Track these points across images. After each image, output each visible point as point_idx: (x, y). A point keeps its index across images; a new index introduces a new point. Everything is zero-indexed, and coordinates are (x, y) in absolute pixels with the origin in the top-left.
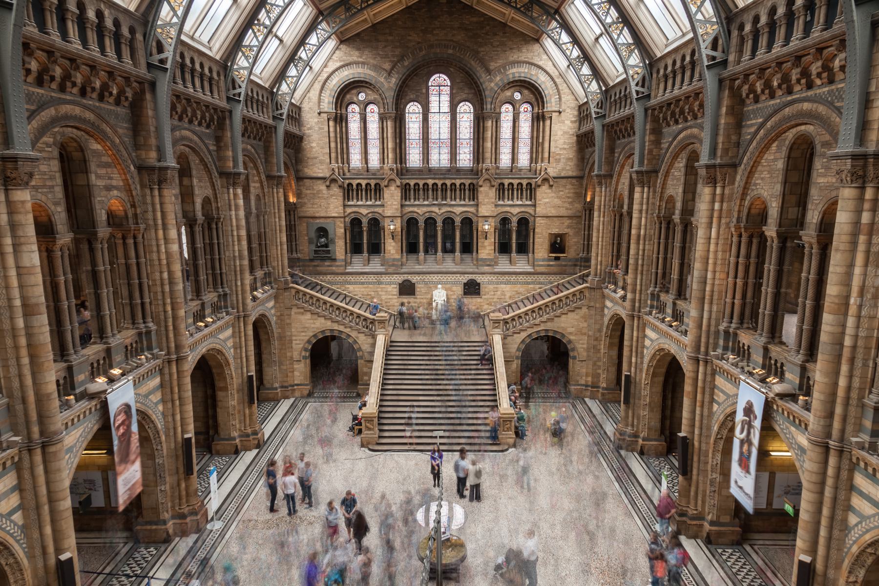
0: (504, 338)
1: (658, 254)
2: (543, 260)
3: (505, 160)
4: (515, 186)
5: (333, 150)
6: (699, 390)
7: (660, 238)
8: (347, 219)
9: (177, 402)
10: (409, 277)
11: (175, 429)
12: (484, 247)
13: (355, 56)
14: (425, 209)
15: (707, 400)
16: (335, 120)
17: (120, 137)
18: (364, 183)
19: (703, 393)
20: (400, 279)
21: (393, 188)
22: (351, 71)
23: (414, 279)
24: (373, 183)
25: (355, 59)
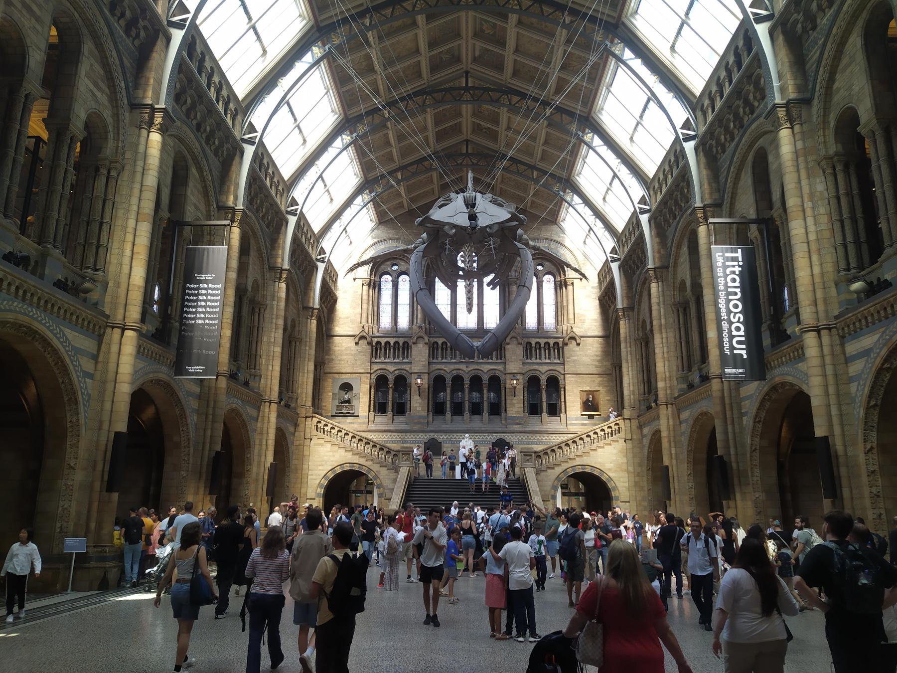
0: (537, 474)
1: (681, 339)
2: (577, 419)
3: (531, 321)
4: (542, 345)
5: (365, 311)
6: (727, 407)
7: (679, 325)
8: (374, 377)
9: (211, 417)
10: (436, 436)
11: (204, 443)
12: (513, 405)
13: (391, 234)
14: (452, 367)
15: (735, 416)
16: (369, 285)
17: (212, 176)
18: (392, 341)
19: (732, 410)
20: (425, 437)
21: (421, 345)
22: (387, 245)
23: (441, 437)
24: (401, 341)
25: (391, 236)
